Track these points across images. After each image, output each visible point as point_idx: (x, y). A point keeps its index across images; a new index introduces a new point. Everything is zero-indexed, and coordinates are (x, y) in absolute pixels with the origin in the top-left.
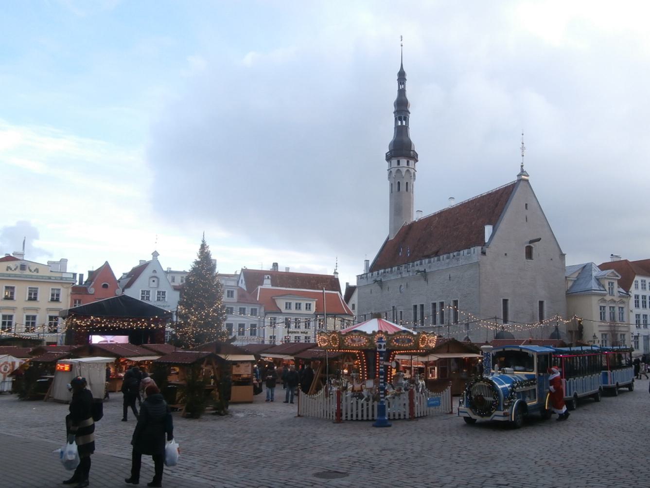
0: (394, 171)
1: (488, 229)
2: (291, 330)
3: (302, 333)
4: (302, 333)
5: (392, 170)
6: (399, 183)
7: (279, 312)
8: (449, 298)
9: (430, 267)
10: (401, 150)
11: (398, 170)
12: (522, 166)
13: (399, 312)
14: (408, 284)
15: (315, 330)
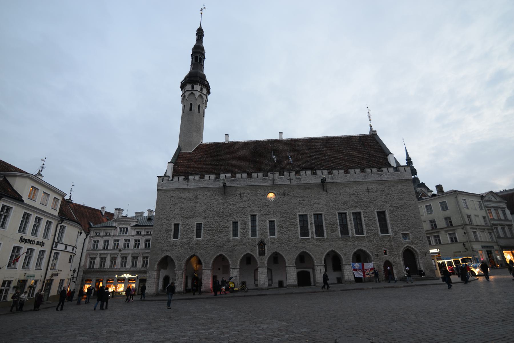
0: (197, 94)
1: (390, 158)
2: (25, 237)
3: (38, 243)
4: (38, 243)
5: (194, 92)
6: (199, 106)
7: (18, 198)
8: (369, 209)
9: (332, 178)
10: (195, 82)
11: (200, 95)
12: (371, 126)
13: (268, 222)
14: (286, 192)
15: (54, 242)
